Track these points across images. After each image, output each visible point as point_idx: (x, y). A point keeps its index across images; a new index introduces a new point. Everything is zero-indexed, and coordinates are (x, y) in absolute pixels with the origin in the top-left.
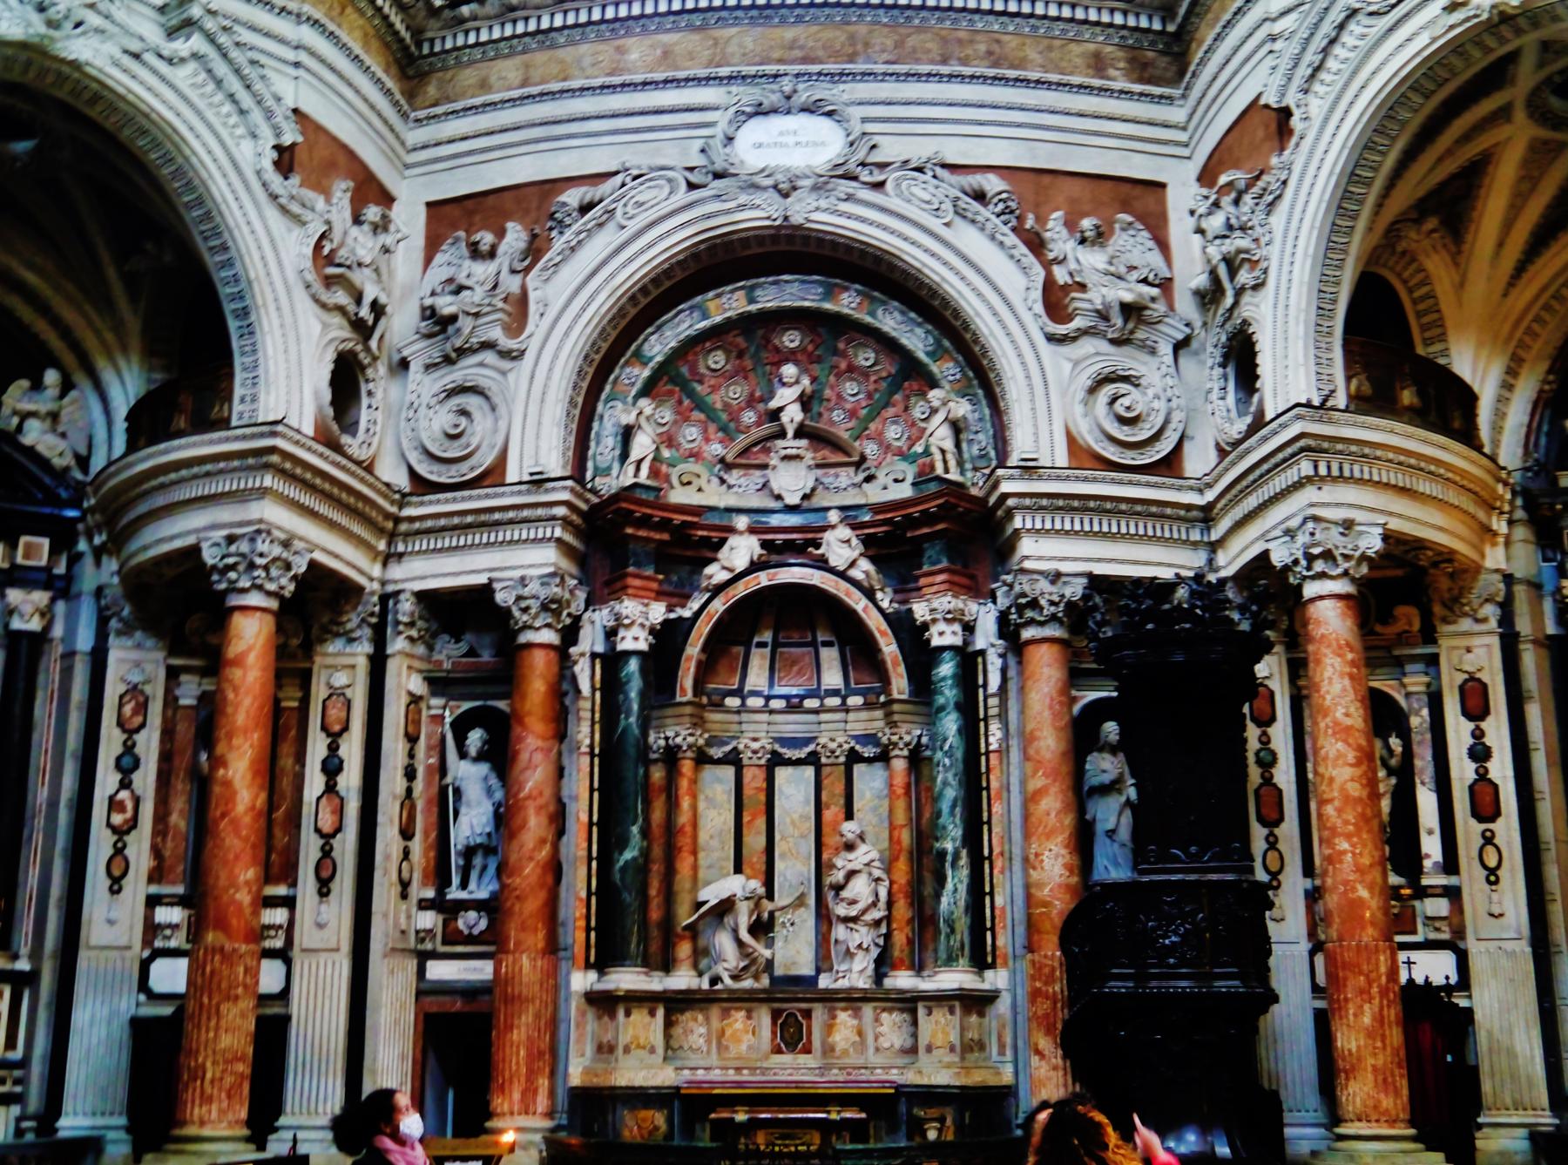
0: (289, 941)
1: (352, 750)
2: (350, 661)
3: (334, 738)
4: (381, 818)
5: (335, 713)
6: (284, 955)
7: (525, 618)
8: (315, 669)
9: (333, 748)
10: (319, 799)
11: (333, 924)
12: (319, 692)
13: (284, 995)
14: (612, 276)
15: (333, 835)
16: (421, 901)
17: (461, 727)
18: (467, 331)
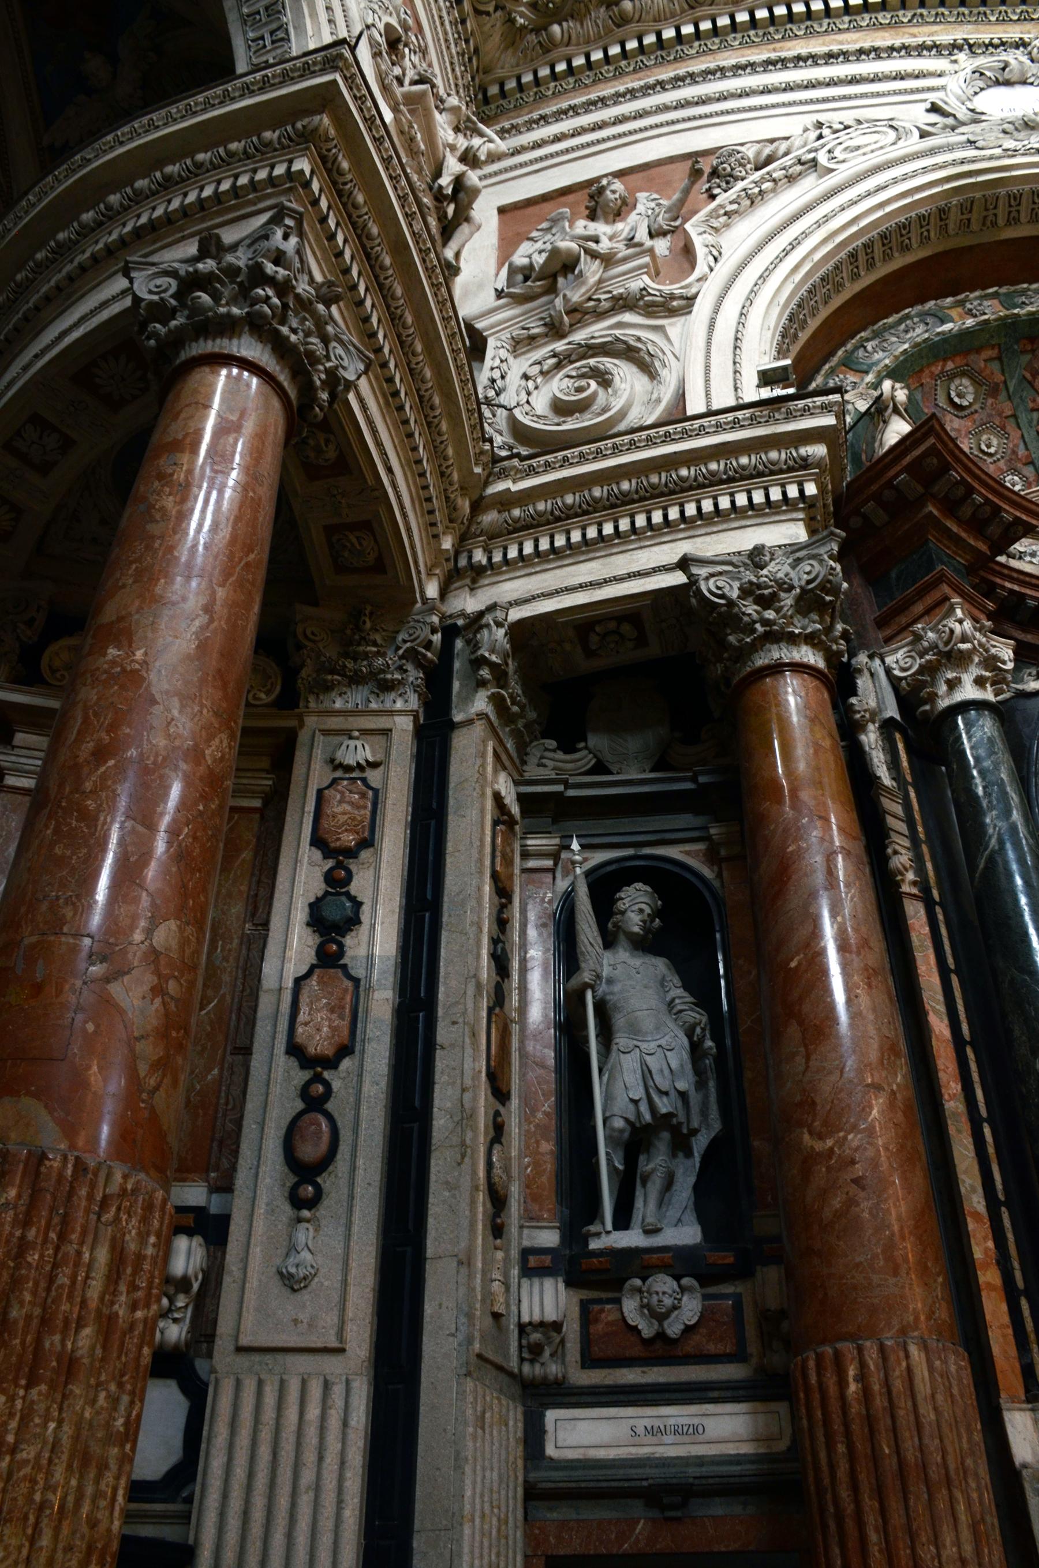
0: (204, 1332)
1: (381, 888)
2: (382, 723)
3: (340, 859)
4: (443, 1033)
5: (343, 808)
6: (179, 1366)
7: (770, 614)
8: (303, 736)
9: (337, 881)
10: (298, 981)
11: (328, 1280)
12: (312, 773)
13: (185, 1473)
14: (827, 218)
15: (332, 1063)
16: (526, 1253)
17: (605, 887)
18: (593, 280)
